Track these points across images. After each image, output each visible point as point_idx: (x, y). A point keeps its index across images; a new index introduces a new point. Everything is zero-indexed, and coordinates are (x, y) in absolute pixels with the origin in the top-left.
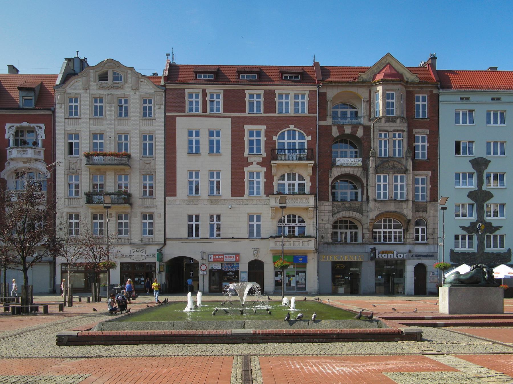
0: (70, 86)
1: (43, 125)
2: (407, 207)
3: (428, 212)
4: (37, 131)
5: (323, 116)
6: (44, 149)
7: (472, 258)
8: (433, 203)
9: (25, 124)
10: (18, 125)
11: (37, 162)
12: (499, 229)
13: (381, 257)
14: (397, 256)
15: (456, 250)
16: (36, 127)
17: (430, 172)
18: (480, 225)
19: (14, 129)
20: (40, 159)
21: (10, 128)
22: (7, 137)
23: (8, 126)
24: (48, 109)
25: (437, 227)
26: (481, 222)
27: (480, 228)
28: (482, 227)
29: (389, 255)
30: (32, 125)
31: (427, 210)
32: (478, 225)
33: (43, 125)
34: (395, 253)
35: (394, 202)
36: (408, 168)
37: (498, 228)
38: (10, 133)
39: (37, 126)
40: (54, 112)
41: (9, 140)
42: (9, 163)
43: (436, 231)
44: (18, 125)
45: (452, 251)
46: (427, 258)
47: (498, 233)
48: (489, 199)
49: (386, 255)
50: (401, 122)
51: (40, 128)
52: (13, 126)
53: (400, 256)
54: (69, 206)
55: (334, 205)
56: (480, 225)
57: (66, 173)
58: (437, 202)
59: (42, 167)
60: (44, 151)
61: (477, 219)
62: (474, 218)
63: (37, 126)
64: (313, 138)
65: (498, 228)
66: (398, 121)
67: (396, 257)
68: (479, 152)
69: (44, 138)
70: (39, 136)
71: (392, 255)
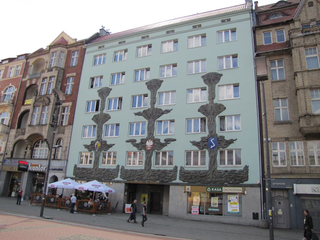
2: (45, 130)
3: (65, 134)
5: (24, 76)
7: (88, 172)
8: (69, 126)
12: (112, 147)
13: (31, 170)
14: (40, 169)
15: (80, 166)
17: (71, 103)
18: (97, 143)
25: (68, 145)
26: (99, 141)
27: (97, 145)
28: (99, 145)
29: (36, 167)
31: (64, 132)
32: (96, 143)
34: (40, 166)
35: (39, 126)
36: (51, 101)
37: (111, 146)
43: (68, 148)
45: (76, 166)
46: (58, 171)
47: (110, 150)
48: (107, 121)
49: (34, 167)
50: (56, 70)
53: (42, 169)
55: (18, 131)
56: (97, 143)
58: (72, 126)
61: (96, 138)
62: (94, 138)
64: (17, 90)
65: (111, 146)
66: (54, 69)
67: (39, 170)
68: (106, 83)
71: (37, 167)
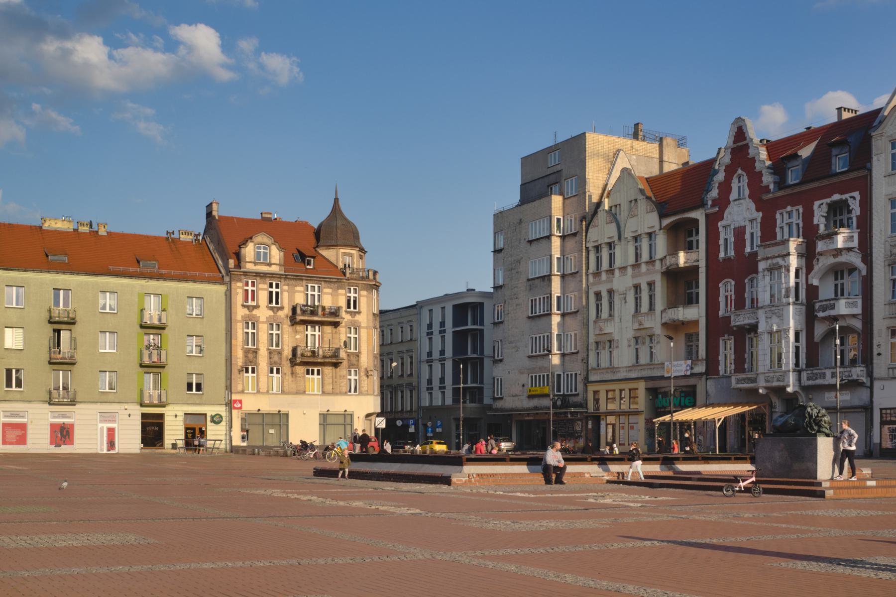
0: (890, 123)
1: (856, 194)
4: (850, 204)
6: (859, 230)
9: (836, 197)
10: (828, 200)
11: (851, 253)
16: (849, 199)
19: (825, 208)
20: (853, 248)
21: (819, 207)
22: (815, 222)
23: (817, 203)
24: (861, 168)
30: (844, 197)
33: (856, 194)
38: (819, 214)
39: (851, 197)
40: (870, 170)
41: (818, 225)
42: (818, 260)
44: (828, 200)
51: (854, 198)
52: (822, 204)
54: (891, 316)
57: (887, 264)
59: (856, 259)
60: (859, 233)
63: (851, 197)
69: (858, 213)
70: (853, 212)
